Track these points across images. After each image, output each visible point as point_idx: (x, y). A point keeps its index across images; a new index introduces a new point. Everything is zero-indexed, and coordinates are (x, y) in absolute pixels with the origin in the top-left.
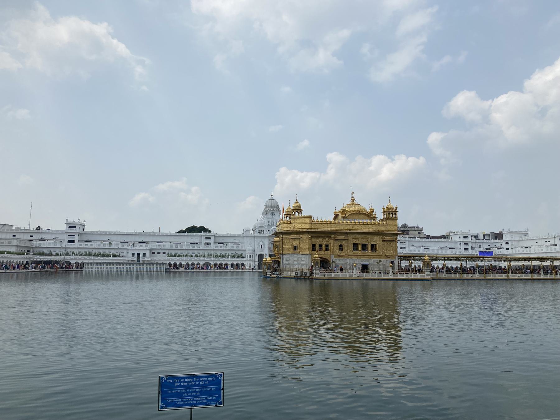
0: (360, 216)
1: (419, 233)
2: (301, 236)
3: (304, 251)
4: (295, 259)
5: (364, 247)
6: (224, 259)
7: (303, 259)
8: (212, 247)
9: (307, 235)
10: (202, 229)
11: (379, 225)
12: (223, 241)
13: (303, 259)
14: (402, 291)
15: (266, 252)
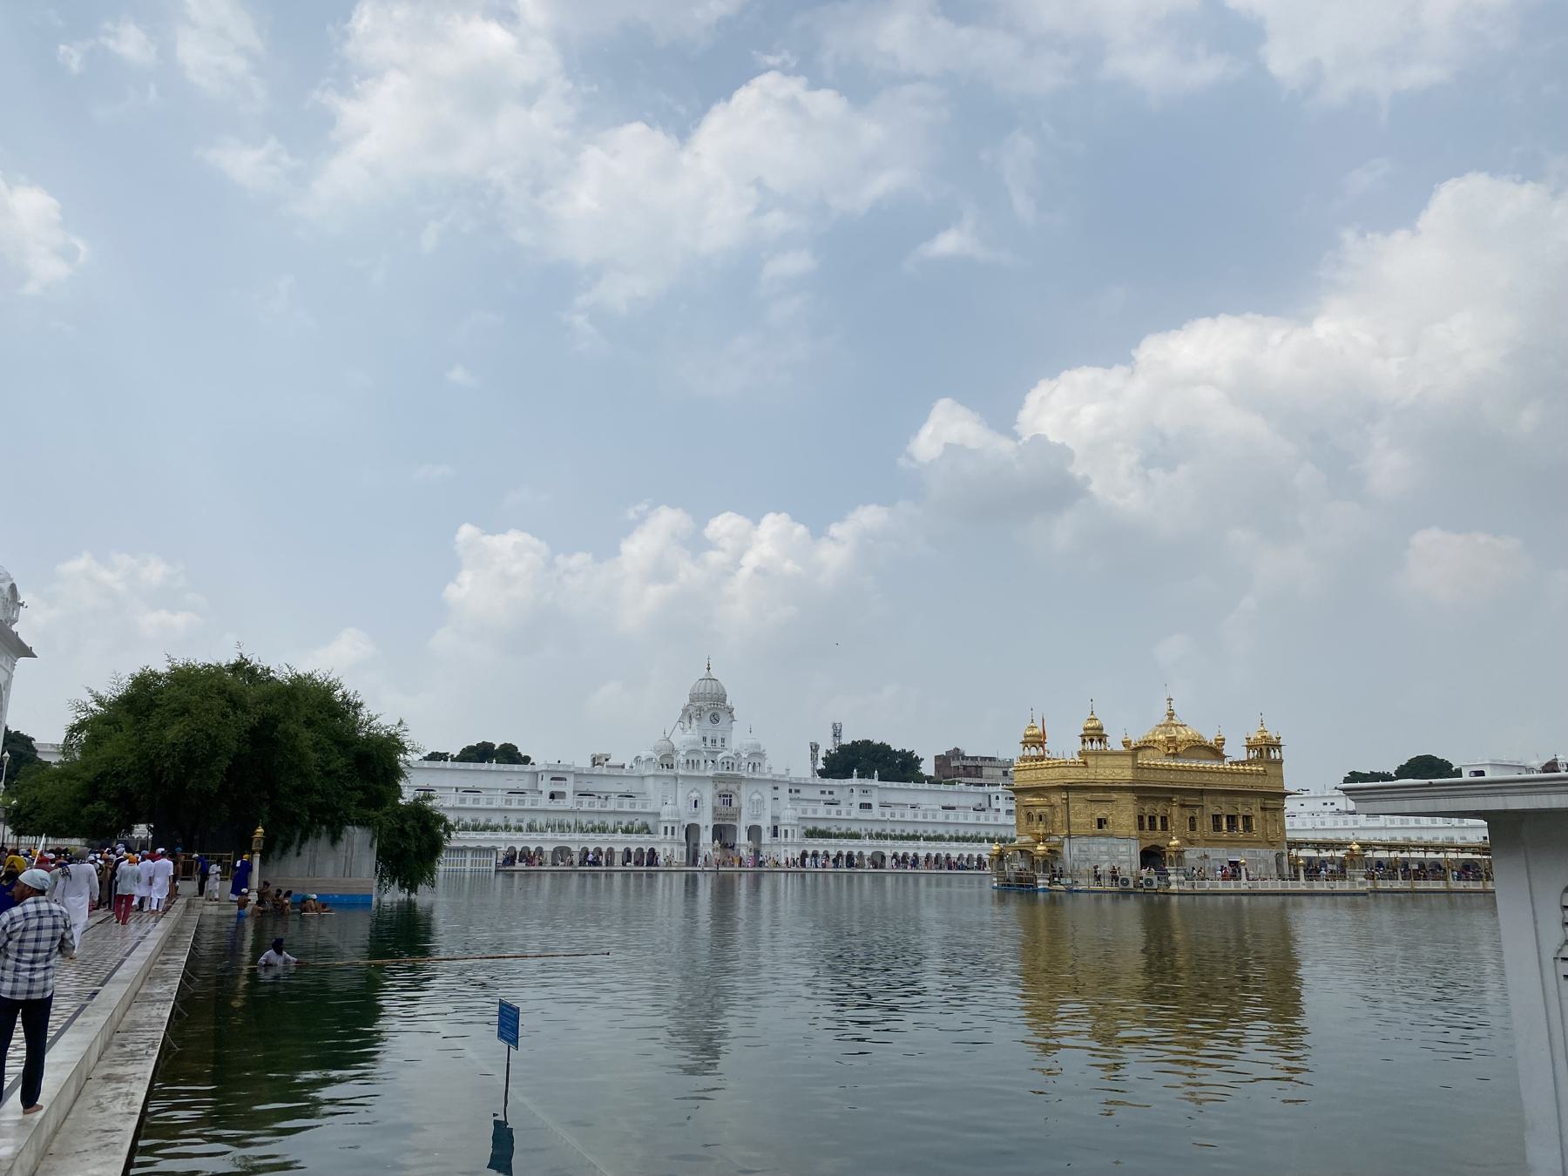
0: (1202, 753)
1: (1005, 774)
2: (1115, 796)
3: (1125, 831)
4: (1103, 849)
5: (1232, 820)
6: (605, 836)
7: (1123, 849)
8: (569, 802)
9: (1131, 796)
10: (509, 755)
11: (1232, 773)
12: (591, 788)
13: (1123, 849)
14: (1293, 913)
15: (706, 821)
